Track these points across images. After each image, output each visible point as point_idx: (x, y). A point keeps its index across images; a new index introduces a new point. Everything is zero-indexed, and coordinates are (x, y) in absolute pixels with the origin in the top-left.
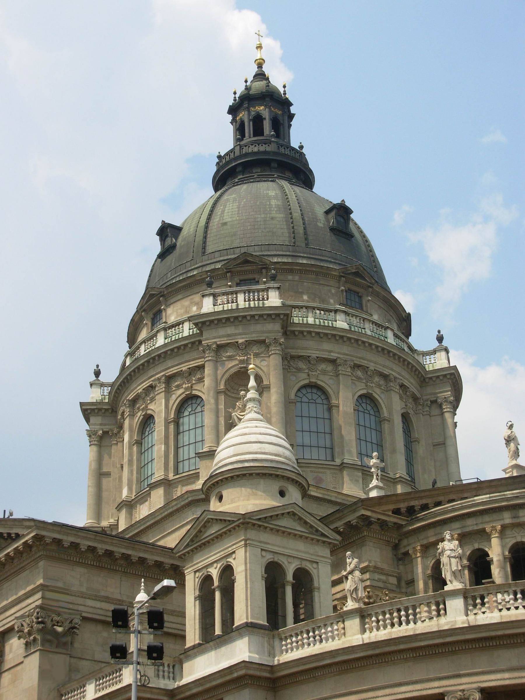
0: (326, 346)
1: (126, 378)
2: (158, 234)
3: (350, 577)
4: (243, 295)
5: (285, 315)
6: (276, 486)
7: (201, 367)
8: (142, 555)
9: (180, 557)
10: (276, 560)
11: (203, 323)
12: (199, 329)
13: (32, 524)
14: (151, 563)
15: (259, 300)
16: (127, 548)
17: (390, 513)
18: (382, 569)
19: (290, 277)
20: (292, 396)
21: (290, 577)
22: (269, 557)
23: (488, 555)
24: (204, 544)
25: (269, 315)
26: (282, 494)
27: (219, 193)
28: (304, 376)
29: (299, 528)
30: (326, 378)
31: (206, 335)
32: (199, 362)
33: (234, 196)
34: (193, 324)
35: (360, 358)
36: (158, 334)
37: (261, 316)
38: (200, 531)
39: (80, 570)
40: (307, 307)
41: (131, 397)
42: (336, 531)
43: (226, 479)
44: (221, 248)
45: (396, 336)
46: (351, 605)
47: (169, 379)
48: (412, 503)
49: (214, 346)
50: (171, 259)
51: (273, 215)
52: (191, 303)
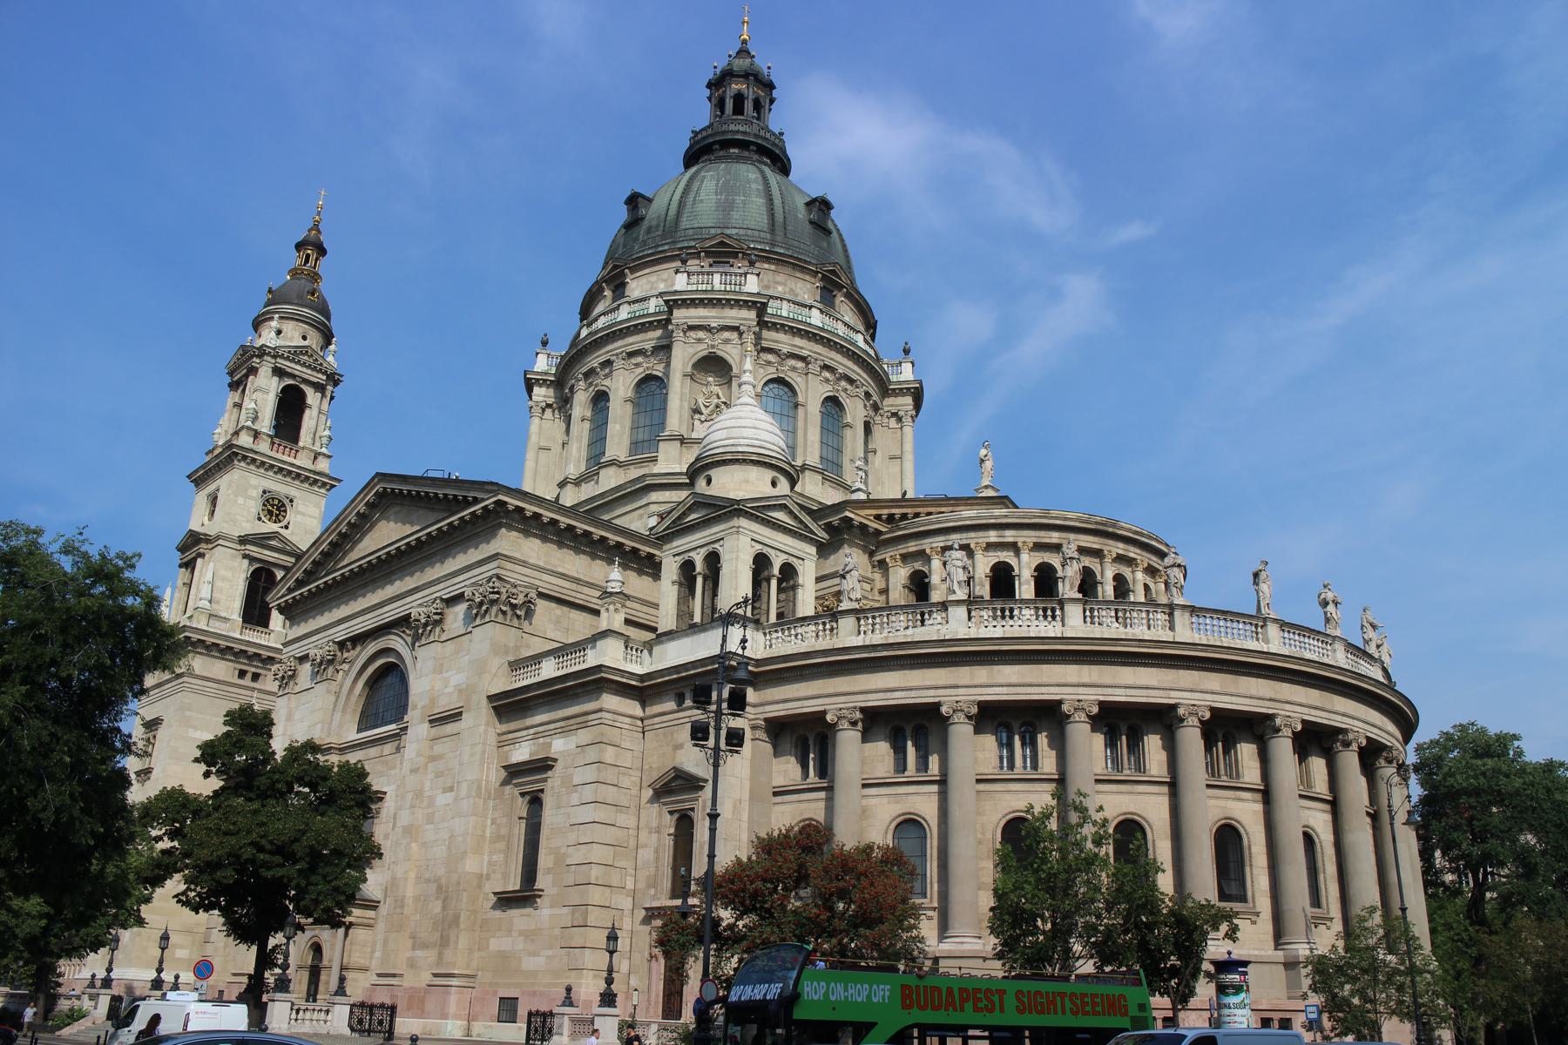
0: (798, 341)
1: (580, 350)
2: (626, 203)
3: (848, 576)
4: (719, 275)
5: (762, 303)
6: (769, 474)
8: (603, 533)
11: (675, 301)
14: (612, 543)
17: (872, 518)
19: (766, 266)
20: (759, 390)
21: (776, 571)
25: (746, 302)
26: (774, 484)
31: (677, 313)
37: (737, 301)
40: (782, 299)
41: (584, 370)
44: (696, 226)
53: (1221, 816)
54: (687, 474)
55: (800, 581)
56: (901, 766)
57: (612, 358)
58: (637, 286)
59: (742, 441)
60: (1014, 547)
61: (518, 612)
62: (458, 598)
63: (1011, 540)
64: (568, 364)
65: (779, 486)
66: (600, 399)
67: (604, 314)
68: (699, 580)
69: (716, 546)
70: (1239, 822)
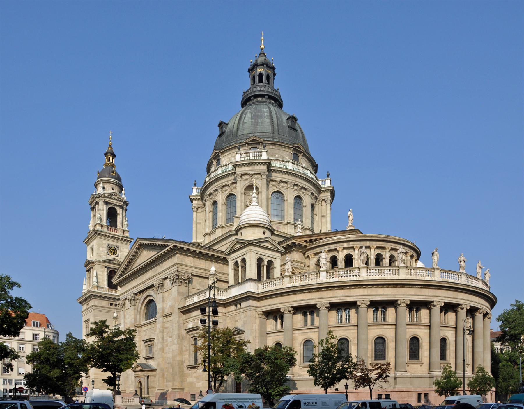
0: (284, 176)
3: (287, 264)
5: (268, 163)
6: (262, 230)
10: (261, 257)
11: (236, 165)
12: (235, 168)
14: (216, 256)
17: (303, 242)
18: (299, 262)
20: (270, 196)
21: (266, 263)
22: (259, 256)
23: (337, 258)
24: (235, 251)
26: (264, 233)
27: (243, 109)
28: (275, 188)
30: (283, 189)
33: (249, 110)
34: (233, 165)
35: (297, 182)
36: (219, 169)
38: (234, 246)
40: (277, 160)
42: (283, 247)
43: (244, 227)
45: (311, 173)
48: (312, 238)
50: (224, 137)
51: (265, 120)
52: (232, 156)
53: (413, 334)
54: (235, 230)
55: (275, 266)
56: (306, 324)
57: (217, 189)
58: (224, 160)
59: (252, 219)
60: (353, 248)
61: (186, 282)
62: (167, 278)
63: (352, 246)
65: (266, 234)
67: (213, 172)
68: (240, 268)
69: (244, 256)
70: (419, 336)
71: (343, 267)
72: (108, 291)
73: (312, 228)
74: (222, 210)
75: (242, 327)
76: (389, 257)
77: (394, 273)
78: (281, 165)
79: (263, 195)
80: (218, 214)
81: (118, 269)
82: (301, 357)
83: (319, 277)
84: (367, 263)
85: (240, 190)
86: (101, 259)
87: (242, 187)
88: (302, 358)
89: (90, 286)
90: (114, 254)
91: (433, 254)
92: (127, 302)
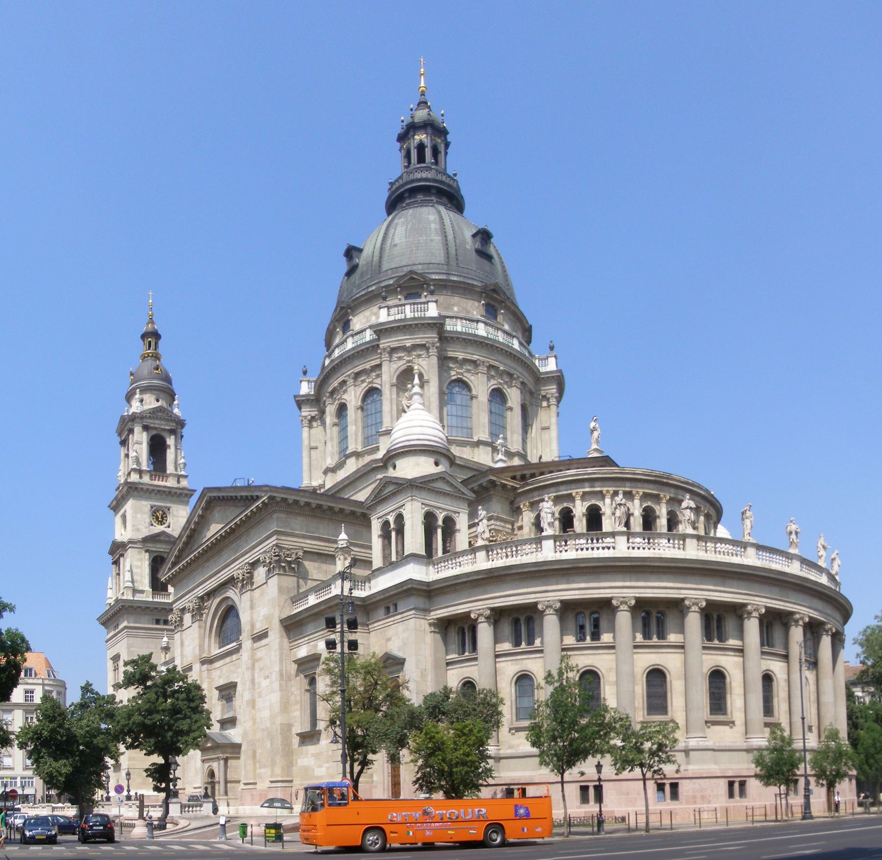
1: (326, 375)
7: (379, 366)
8: (341, 506)
9: (368, 508)
12: (377, 335)
13: (268, 489)
14: (348, 512)
15: (421, 311)
16: (331, 502)
29: (447, 488)
32: (378, 362)
33: (402, 220)
39: (300, 519)
46: (480, 543)
47: (357, 375)
49: (389, 349)
50: (356, 276)
51: (432, 238)
57: (346, 379)
58: (358, 322)
64: (321, 384)
66: (342, 409)
71: (585, 531)
72: (151, 596)
73: (524, 451)
74: (356, 420)
75: (399, 650)
76: (668, 515)
77: (676, 546)
78: (464, 328)
79: (433, 388)
80: (349, 428)
81: (168, 553)
82: (512, 709)
83: (540, 550)
84: (627, 524)
85: (388, 380)
86: (140, 536)
87: (392, 374)
88: (514, 711)
89: (120, 590)
90: (161, 523)
91: (743, 513)
92: (187, 617)
